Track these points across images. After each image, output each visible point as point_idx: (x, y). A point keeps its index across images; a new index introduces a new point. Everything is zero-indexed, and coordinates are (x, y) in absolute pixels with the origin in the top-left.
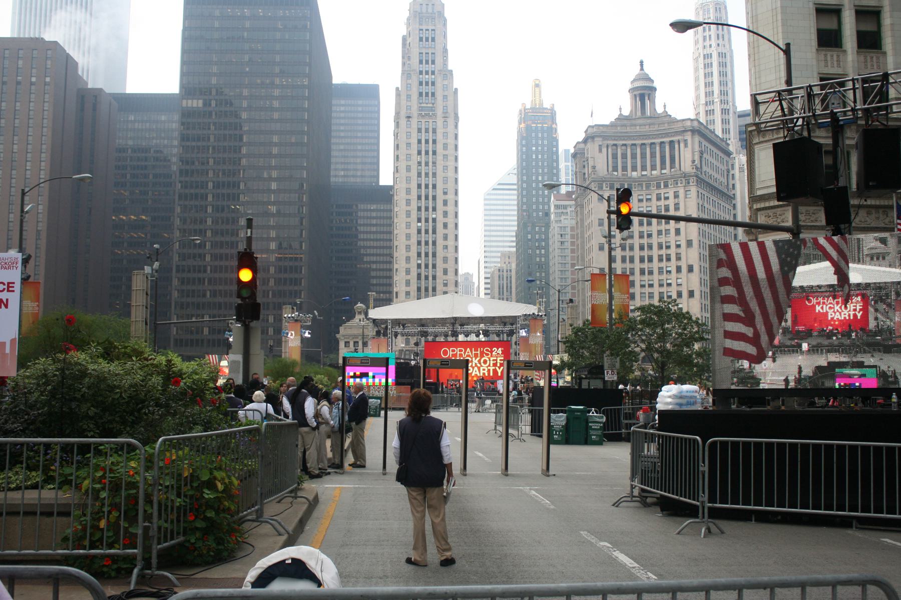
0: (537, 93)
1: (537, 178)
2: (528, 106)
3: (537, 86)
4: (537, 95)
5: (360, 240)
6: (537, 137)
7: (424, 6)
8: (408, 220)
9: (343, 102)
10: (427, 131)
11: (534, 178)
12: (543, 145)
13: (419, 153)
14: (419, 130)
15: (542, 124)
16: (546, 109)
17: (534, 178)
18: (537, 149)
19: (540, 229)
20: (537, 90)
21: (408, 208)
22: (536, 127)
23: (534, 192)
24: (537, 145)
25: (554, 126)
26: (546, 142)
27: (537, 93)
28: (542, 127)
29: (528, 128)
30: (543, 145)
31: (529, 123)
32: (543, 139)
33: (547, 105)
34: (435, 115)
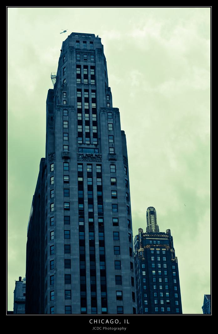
0: (153, 219)
1: (159, 302)
2: (145, 231)
4: (153, 221)
8: (68, 287)
11: (156, 302)
12: (162, 269)
13: (81, 201)
15: (161, 248)
17: (156, 302)
18: (157, 272)
20: (152, 217)
21: (68, 271)
24: (156, 269)
25: (172, 250)
26: (165, 266)
27: (153, 219)
29: (147, 252)
30: (162, 269)
31: (148, 246)
32: (162, 262)
33: (162, 230)
34: (99, 157)
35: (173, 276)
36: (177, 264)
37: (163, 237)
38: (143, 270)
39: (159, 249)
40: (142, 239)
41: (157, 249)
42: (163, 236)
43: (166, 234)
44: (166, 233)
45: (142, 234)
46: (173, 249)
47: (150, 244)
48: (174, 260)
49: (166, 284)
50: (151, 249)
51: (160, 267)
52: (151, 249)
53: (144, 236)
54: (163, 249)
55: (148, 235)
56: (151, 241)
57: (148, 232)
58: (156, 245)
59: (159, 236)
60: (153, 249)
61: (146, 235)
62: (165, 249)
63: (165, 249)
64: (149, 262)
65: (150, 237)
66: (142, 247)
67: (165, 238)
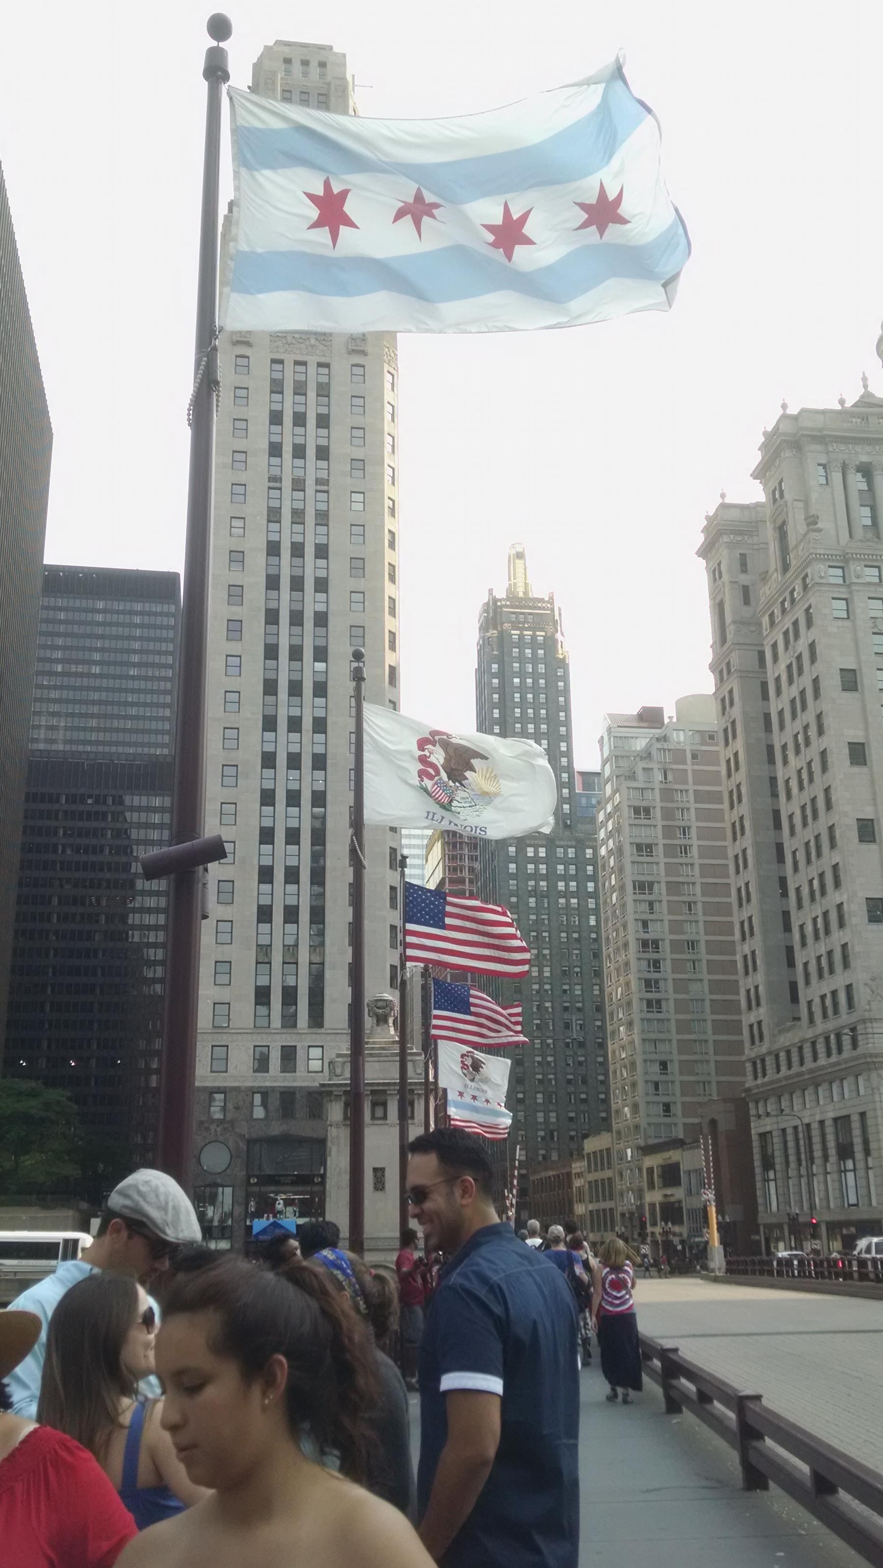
3: (520, 556)
5: (134, 910)
6: (521, 659)
7: (297, 67)
9: (101, 605)
10: (300, 389)
14: (277, 387)
15: (534, 629)
16: (542, 600)
19: (536, 852)
20: (519, 563)
22: (521, 637)
23: (544, 727)
24: (522, 674)
26: (541, 668)
28: (534, 637)
32: (534, 660)
35: (558, 691)
36: (568, 664)
37: (539, 608)
38: (494, 675)
39: (530, 633)
40: (495, 612)
41: (525, 633)
42: (539, 605)
43: (548, 602)
44: (546, 599)
45: (495, 601)
46: (562, 634)
47: (511, 622)
48: (561, 657)
49: (541, 706)
50: (513, 632)
51: (531, 670)
52: (513, 632)
53: (499, 604)
54: (538, 633)
55: (508, 603)
56: (514, 616)
57: (507, 596)
58: (524, 623)
59: (531, 604)
60: (518, 632)
61: (504, 603)
62: (543, 634)
63: (543, 634)
64: (506, 658)
65: (512, 607)
66: (495, 628)
67: (544, 609)
